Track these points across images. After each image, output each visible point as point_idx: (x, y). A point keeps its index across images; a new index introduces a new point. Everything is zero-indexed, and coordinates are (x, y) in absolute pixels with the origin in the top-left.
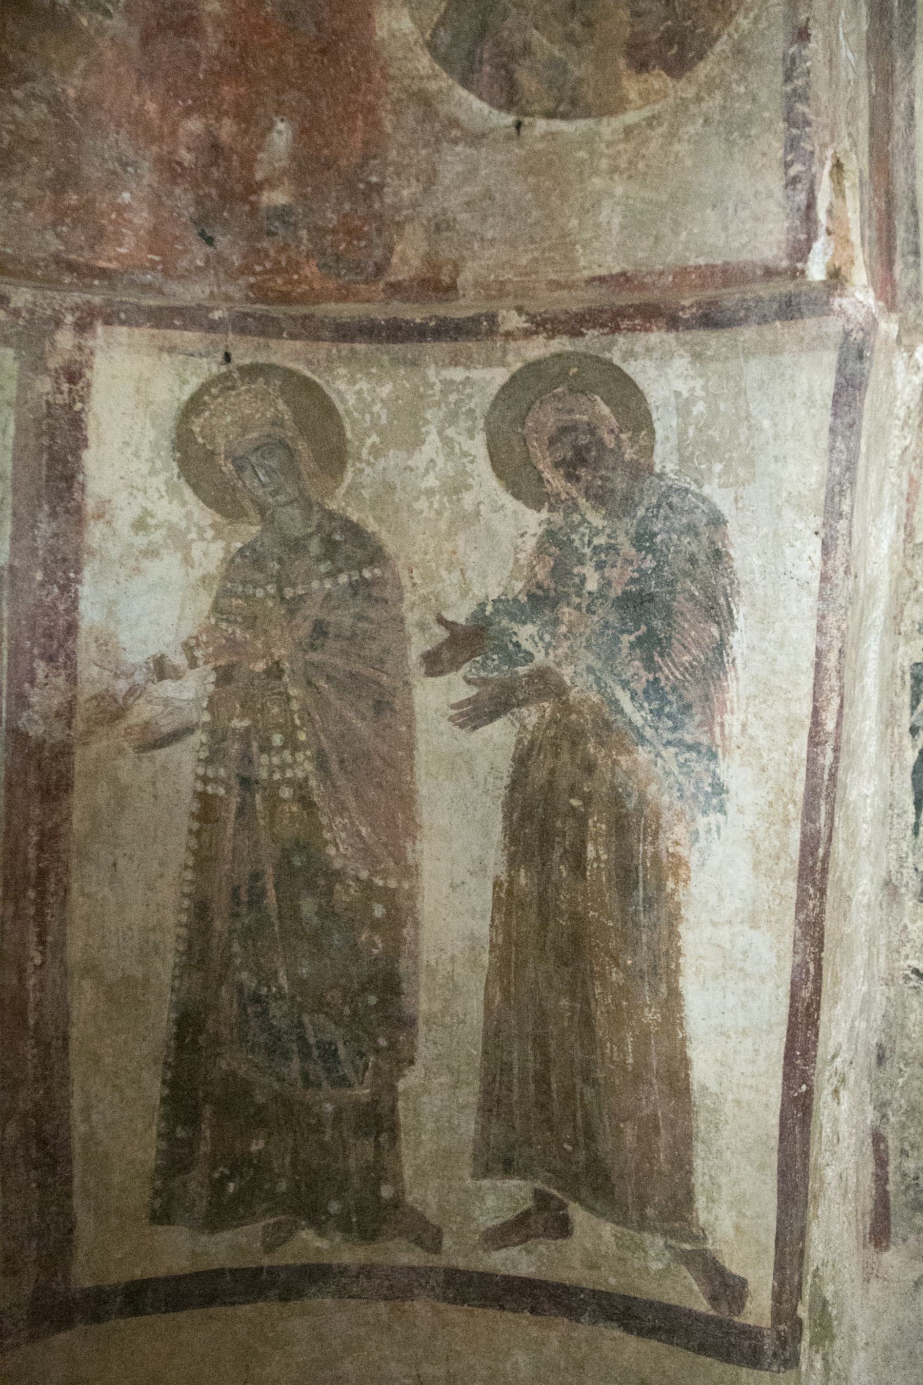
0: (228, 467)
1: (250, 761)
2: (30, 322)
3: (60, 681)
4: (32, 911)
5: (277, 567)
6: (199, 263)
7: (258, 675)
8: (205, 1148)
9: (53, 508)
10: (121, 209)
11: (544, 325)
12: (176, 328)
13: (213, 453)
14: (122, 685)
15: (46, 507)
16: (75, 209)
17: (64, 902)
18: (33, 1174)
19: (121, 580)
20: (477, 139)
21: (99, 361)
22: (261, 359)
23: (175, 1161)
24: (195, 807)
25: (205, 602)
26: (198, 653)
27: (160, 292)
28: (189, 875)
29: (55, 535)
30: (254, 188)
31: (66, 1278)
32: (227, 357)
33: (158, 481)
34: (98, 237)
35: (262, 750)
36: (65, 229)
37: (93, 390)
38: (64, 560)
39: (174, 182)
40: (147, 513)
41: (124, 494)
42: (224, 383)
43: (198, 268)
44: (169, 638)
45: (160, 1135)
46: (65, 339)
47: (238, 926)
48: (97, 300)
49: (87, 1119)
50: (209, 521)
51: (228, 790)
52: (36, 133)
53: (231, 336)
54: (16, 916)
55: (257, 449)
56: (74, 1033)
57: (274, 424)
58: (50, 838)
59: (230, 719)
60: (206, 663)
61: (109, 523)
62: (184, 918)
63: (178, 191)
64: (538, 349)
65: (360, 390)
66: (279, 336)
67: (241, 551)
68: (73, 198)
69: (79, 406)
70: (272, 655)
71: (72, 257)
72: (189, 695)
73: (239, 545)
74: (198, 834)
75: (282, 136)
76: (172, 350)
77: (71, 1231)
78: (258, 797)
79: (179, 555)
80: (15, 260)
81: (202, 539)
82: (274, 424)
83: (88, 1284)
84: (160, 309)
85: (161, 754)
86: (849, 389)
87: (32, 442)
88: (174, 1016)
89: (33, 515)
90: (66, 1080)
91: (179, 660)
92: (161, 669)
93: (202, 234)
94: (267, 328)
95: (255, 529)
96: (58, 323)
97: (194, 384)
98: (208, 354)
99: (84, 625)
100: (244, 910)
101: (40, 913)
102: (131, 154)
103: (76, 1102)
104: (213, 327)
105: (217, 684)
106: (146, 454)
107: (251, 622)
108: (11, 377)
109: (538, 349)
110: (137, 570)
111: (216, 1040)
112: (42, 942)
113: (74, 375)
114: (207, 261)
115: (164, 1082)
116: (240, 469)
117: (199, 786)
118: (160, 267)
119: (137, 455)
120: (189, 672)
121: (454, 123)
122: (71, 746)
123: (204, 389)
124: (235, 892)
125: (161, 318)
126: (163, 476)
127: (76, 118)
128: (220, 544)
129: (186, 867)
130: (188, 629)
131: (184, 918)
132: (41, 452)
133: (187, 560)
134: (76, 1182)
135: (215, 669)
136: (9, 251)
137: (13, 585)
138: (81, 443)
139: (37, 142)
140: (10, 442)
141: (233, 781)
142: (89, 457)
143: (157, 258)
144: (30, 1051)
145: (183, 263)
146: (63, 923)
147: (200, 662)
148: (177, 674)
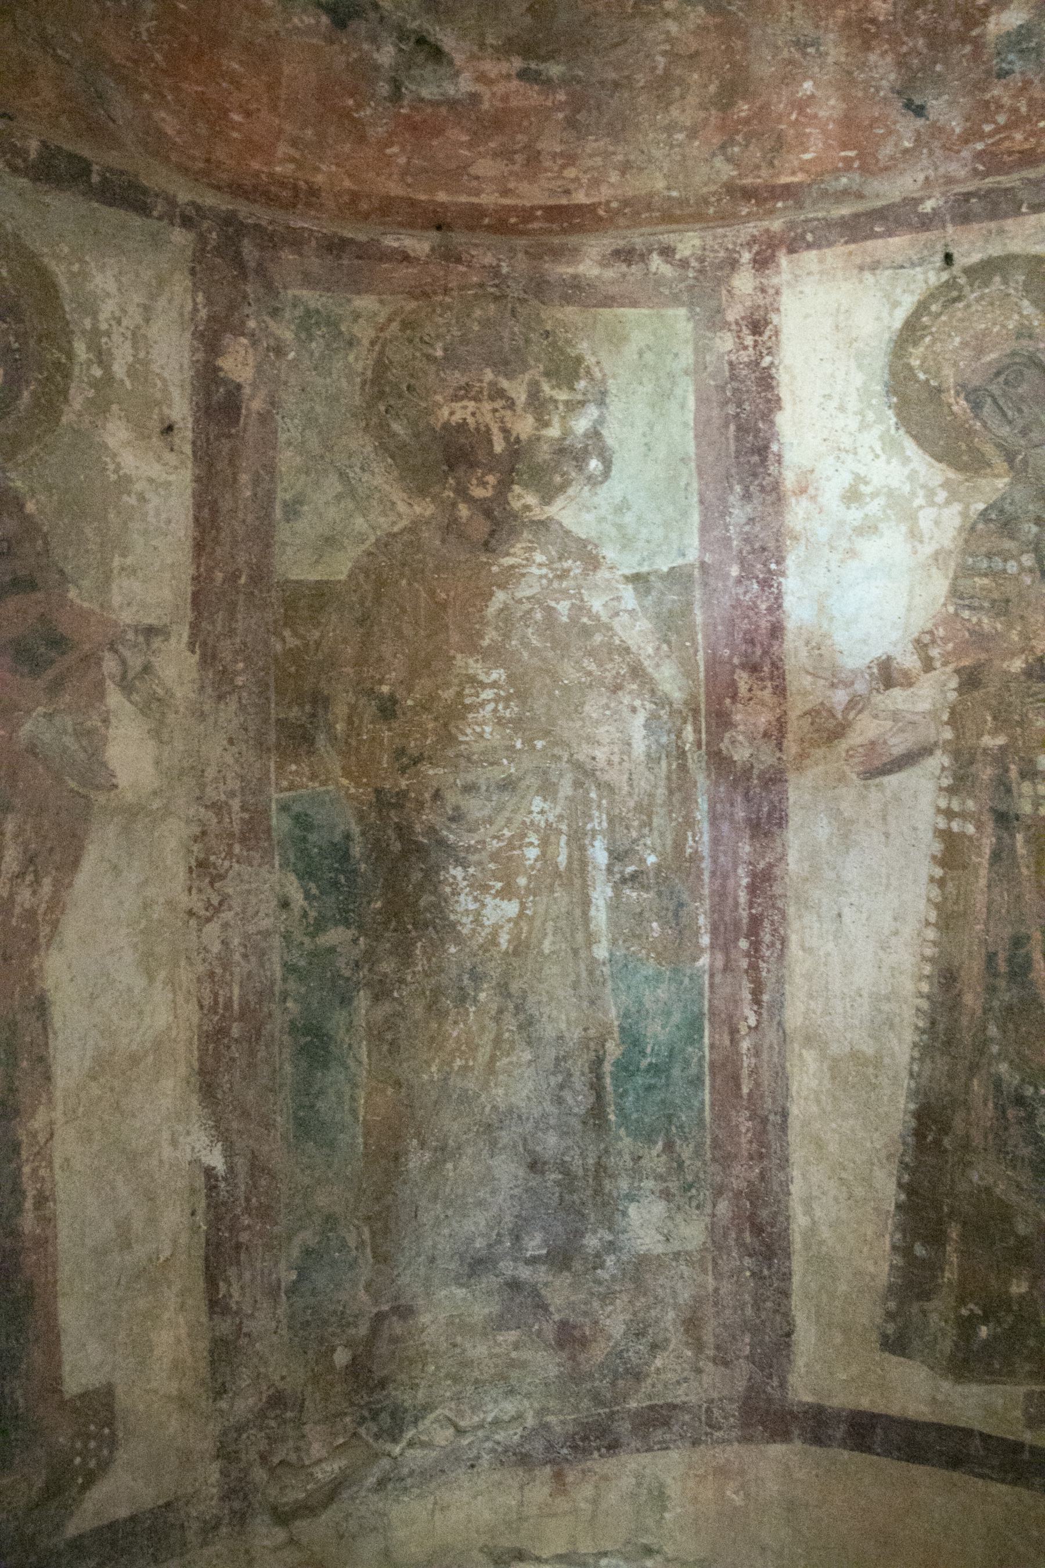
0: (961, 406)
1: (1009, 791)
2: (701, 271)
3: (767, 694)
4: (744, 963)
5: (1035, 529)
6: (907, 144)
7: (1016, 677)
8: (950, 1275)
9: (746, 489)
10: (801, 105)
12: (879, 236)
13: (939, 390)
14: (840, 697)
15: (738, 488)
16: (747, 121)
17: (781, 957)
18: (747, 1261)
19: (833, 566)
21: (787, 301)
22: (995, 250)
23: (913, 1282)
24: (937, 847)
25: (940, 586)
26: (935, 652)
27: (860, 196)
28: (931, 934)
29: (751, 520)
31: (783, 1384)
32: (948, 258)
33: (871, 438)
34: (779, 144)
35: (1023, 775)
36: (736, 149)
37: (783, 337)
38: (764, 549)
39: (867, 47)
40: (859, 479)
41: (831, 459)
42: (948, 294)
43: (906, 151)
44: (895, 635)
45: (894, 1248)
46: (744, 282)
47: (996, 1004)
48: (776, 225)
49: (809, 1211)
50: (939, 479)
51: (979, 826)
52: (694, 46)
53: (950, 229)
54: (726, 968)
55: (998, 374)
56: (794, 1110)
57: (1019, 336)
58: (762, 881)
59: (979, 736)
60: (945, 664)
61: (813, 498)
62: (925, 987)
63: (873, 57)
66: (1017, 212)
67: (984, 514)
68: (743, 109)
69: (767, 361)
70: (1032, 649)
71: (747, 181)
72: (925, 706)
73: (981, 506)
74: (941, 883)
76: (875, 266)
77: (788, 1335)
78: (1020, 837)
79: (904, 528)
80: (682, 202)
81: (932, 504)
82: (1019, 336)
83: (808, 1398)
84: (857, 216)
85: (892, 781)
87: (715, 413)
88: (912, 1106)
89: (723, 500)
90: (784, 1163)
91: (910, 661)
92: (887, 675)
93: (909, 105)
94: (997, 206)
95: (1002, 483)
96: (733, 264)
97: (908, 303)
98: (922, 261)
99: (790, 625)
100: (1002, 983)
101: (754, 967)
102: (809, 30)
103: (796, 1189)
104: (926, 223)
105: (960, 689)
106: (853, 404)
107: (1002, 607)
108: (687, 342)
110: (852, 553)
111: (966, 1145)
112: (757, 1001)
113: (757, 325)
114: (918, 140)
115: (900, 1185)
116: (976, 406)
117: (942, 824)
118: (856, 165)
119: (842, 409)
120: (924, 677)
122: (782, 772)
123: (922, 308)
124: (991, 957)
125: (856, 229)
126: (877, 430)
127: (740, 9)
128: (957, 507)
129: (928, 924)
130: (920, 622)
131: (925, 987)
132: (726, 426)
133: (914, 535)
134: (796, 1279)
135: (957, 671)
136: (675, 194)
137: (706, 584)
138: (774, 404)
139: (697, 53)
140: (690, 417)
141: (987, 817)
142: (783, 420)
143: (852, 154)
144: (745, 1125)
145: (886, 151)
146: (780, 981)
147: (937, 664)
148: (908, 681)
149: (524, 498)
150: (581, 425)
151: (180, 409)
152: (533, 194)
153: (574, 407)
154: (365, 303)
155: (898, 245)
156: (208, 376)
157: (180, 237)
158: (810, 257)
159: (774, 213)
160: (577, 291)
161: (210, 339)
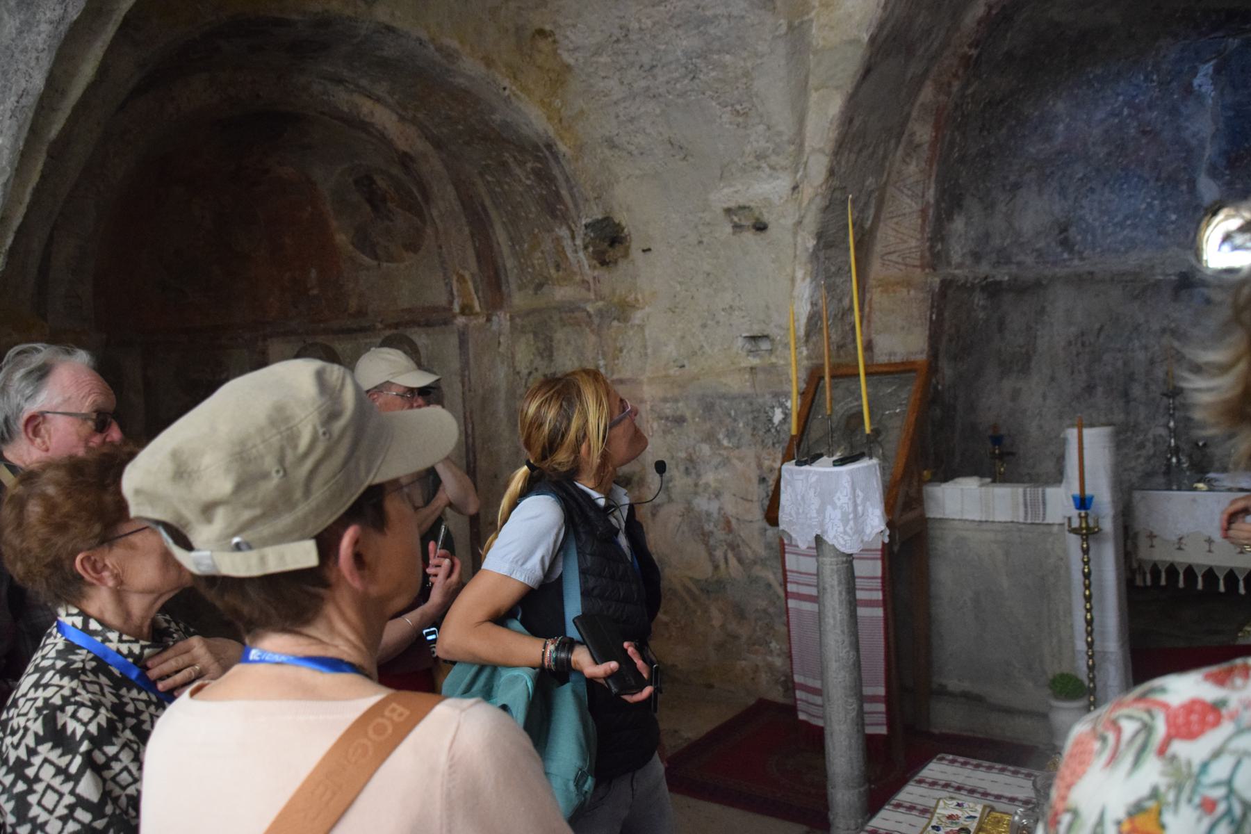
11: (389, 326)
20: (368, 269)
46: (260, 344)
64: (388, 333)
75: (314, 274)
86: (463, 343)
109: (388, 333)
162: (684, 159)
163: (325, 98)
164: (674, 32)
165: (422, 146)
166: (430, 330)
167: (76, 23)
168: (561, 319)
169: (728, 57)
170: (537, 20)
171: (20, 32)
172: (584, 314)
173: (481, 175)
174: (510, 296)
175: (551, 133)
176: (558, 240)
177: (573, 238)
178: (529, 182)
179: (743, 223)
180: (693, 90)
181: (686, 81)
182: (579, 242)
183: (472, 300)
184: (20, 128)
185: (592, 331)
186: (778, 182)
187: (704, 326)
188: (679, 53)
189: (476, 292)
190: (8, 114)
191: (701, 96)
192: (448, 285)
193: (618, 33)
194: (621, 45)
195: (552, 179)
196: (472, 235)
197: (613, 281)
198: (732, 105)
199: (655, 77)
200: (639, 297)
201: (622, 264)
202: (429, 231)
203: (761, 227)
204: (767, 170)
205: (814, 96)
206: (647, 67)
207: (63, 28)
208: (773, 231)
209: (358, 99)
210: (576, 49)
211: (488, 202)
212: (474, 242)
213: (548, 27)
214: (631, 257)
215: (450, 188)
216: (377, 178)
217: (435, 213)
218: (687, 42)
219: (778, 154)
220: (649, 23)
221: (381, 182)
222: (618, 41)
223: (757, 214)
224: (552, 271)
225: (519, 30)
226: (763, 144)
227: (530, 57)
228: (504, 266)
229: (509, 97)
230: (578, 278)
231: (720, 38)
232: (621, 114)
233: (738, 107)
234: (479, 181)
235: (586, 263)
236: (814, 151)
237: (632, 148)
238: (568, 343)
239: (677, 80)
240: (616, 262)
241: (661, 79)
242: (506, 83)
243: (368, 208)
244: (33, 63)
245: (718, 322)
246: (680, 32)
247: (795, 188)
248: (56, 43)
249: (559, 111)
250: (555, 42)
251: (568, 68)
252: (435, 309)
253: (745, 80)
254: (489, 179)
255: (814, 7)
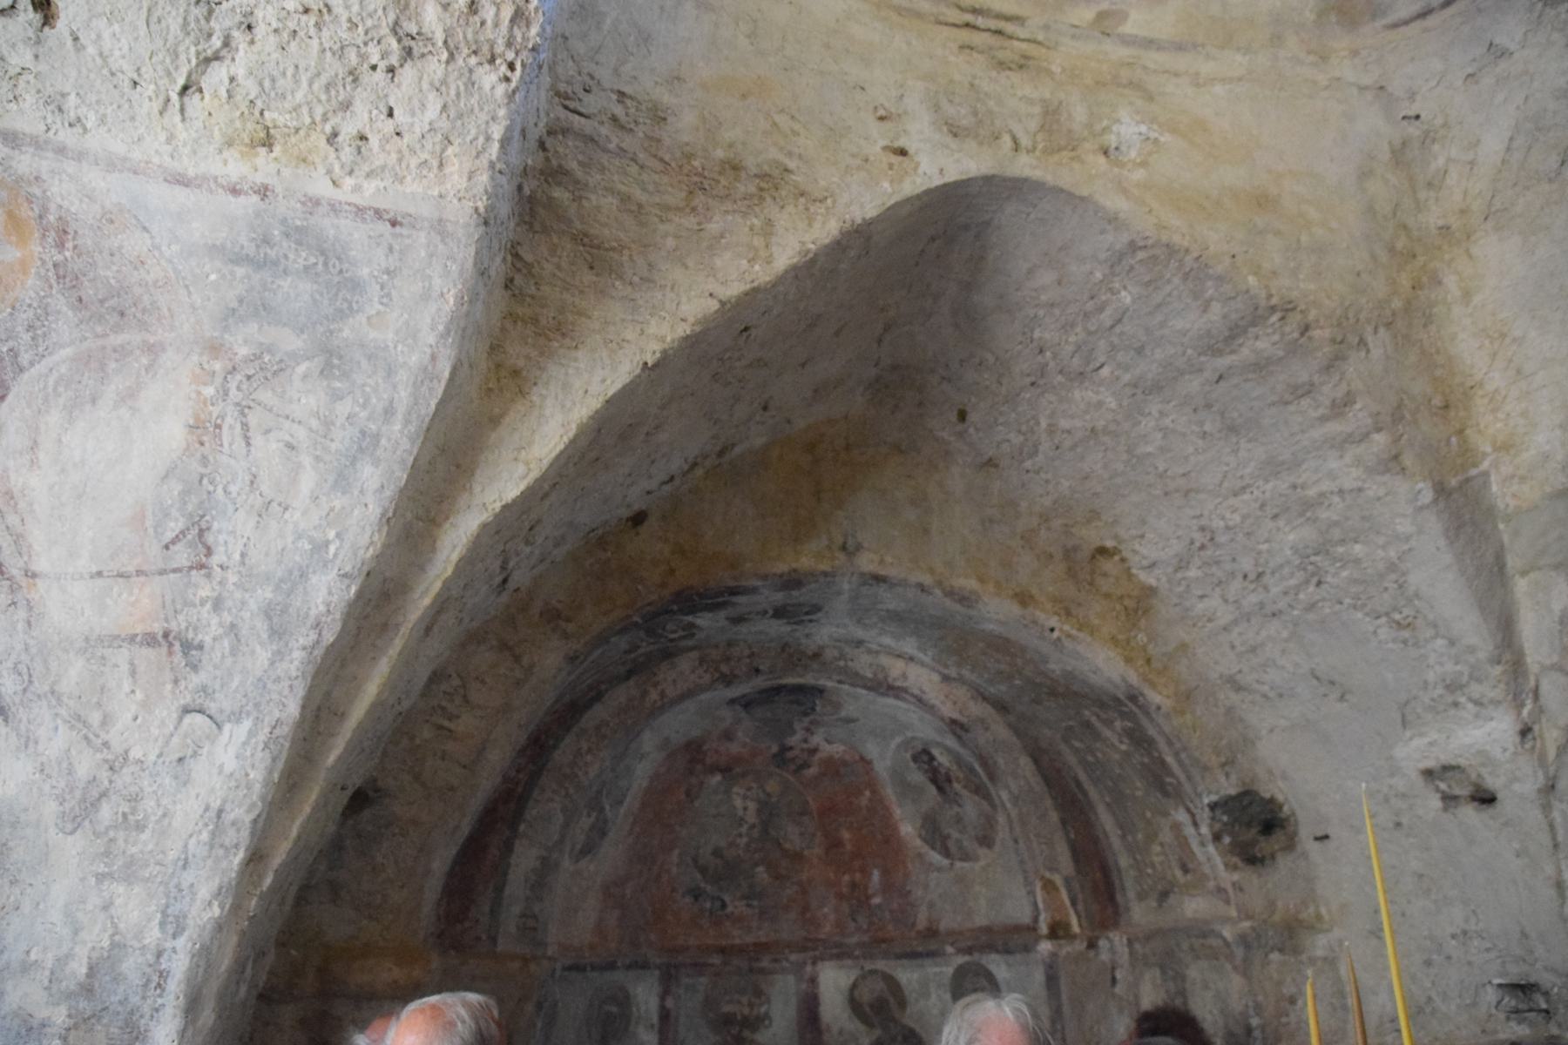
0: (867, 1009)
20: (939, 869)
30: (868, 898)
42: (863, 977)
46: (809, 968)
65: (907, 976)
68: (808, 915)
75: (876, 875)
97: (852, 978)
113: (813, 981)
121: (931, 864)
125: (839, 957)
149: (746, 1033)
150: (763, 1010)
151: (655, 1019)
152: (749, 939)
153: (761, 1005)
154: (702, 979)
155: (849, 962)
156: (662, 1008)
157: (657, 972)
158: (827, 964)
159: (818, 948)
160: (762, 971)
161: (663, 998)
162: (1342, 698)
163: (842, 663)
164: (1271, 524)
165: (977, 709)
166: (1011, 958)
167: (332, 645)
168: (1192, 949)
169: (1358, 548)
170: (1092, 536)
171: (272, 663)
172: (1220, 942)
173: (1066, 740)
174: (1128, 909)
175: (1133, 678)
176: (1177, 827)
177: (1196, 824)
178: (1124, 747)
179: (1457, 791)
180: (1324, 599)
181: (1311, 588)
182: (1204, 830)
183: (1067, 915)
184: (274, 760)
185: (1235, 968)
186: (1493, 724)
187: (1428, 963)
188: (1289, 552)
189: (1074, 903)
190: (261, 746)
191: (1338, 607)
192: (1031, 893)
193: (1199, 538)
194: (1209, 553)
195: (1151, 742)
196: (1064, 822)
197: (1274, 887)
198: (1387, 614)
199: (1266, 588)
200: (1323, 911)
201: (1284, 863)
202: (1001, 819)
203: (1485, 799)
204: (1470, 706)
205: (1521, 586)
206: (1252, 576)
207: (319, 652)
208: (1506, 805)
209: (885, 660)
210: (1153, 565)
211: (1082, 777)
212: (1067, 834)
213: (1109, 544)
214: (1299, 849)
215: (1025, 762)
216: (936, 752)
217: (1005, 795)
218: (1293, 536)
219: (1479, 681)
220: (1237, 518)
221: (942, 759)
222: (1202, 547)
223: (1473, 776)
224: (1178, 873)
225: (1069, 553)
226: (1450, 667)
227: (1091, 584)
228: (1116, 862)
229: (1059, 639)
230: (1211, 884)
231: (1336, 524)
232: (1237, 643)
233: (1397, 617)
234: (1063, 747)
235: (1218, 861)
236: (1545, 669)
237: (1266, 688)
238: (1206, 987)
239: (1298, 589)
240: (1273, 857)
241: (1275, 590)
242: (1053, 621)
243: (933, 790)
244: (286, 692)
245: (1449, 958)
246: (1281, 523)
247: (1525, 732)
248: (311, 669)
249: (1144, 648)
250: (1123, 560)
251: (1151, 591)
252: (1017, 929)
253: (1393, 577)
254: (1077, 744)
255: (1485, 455)
